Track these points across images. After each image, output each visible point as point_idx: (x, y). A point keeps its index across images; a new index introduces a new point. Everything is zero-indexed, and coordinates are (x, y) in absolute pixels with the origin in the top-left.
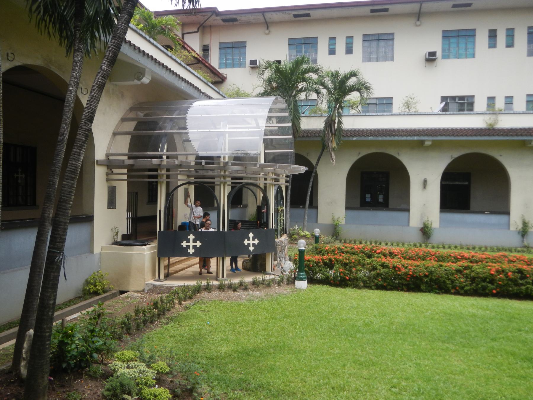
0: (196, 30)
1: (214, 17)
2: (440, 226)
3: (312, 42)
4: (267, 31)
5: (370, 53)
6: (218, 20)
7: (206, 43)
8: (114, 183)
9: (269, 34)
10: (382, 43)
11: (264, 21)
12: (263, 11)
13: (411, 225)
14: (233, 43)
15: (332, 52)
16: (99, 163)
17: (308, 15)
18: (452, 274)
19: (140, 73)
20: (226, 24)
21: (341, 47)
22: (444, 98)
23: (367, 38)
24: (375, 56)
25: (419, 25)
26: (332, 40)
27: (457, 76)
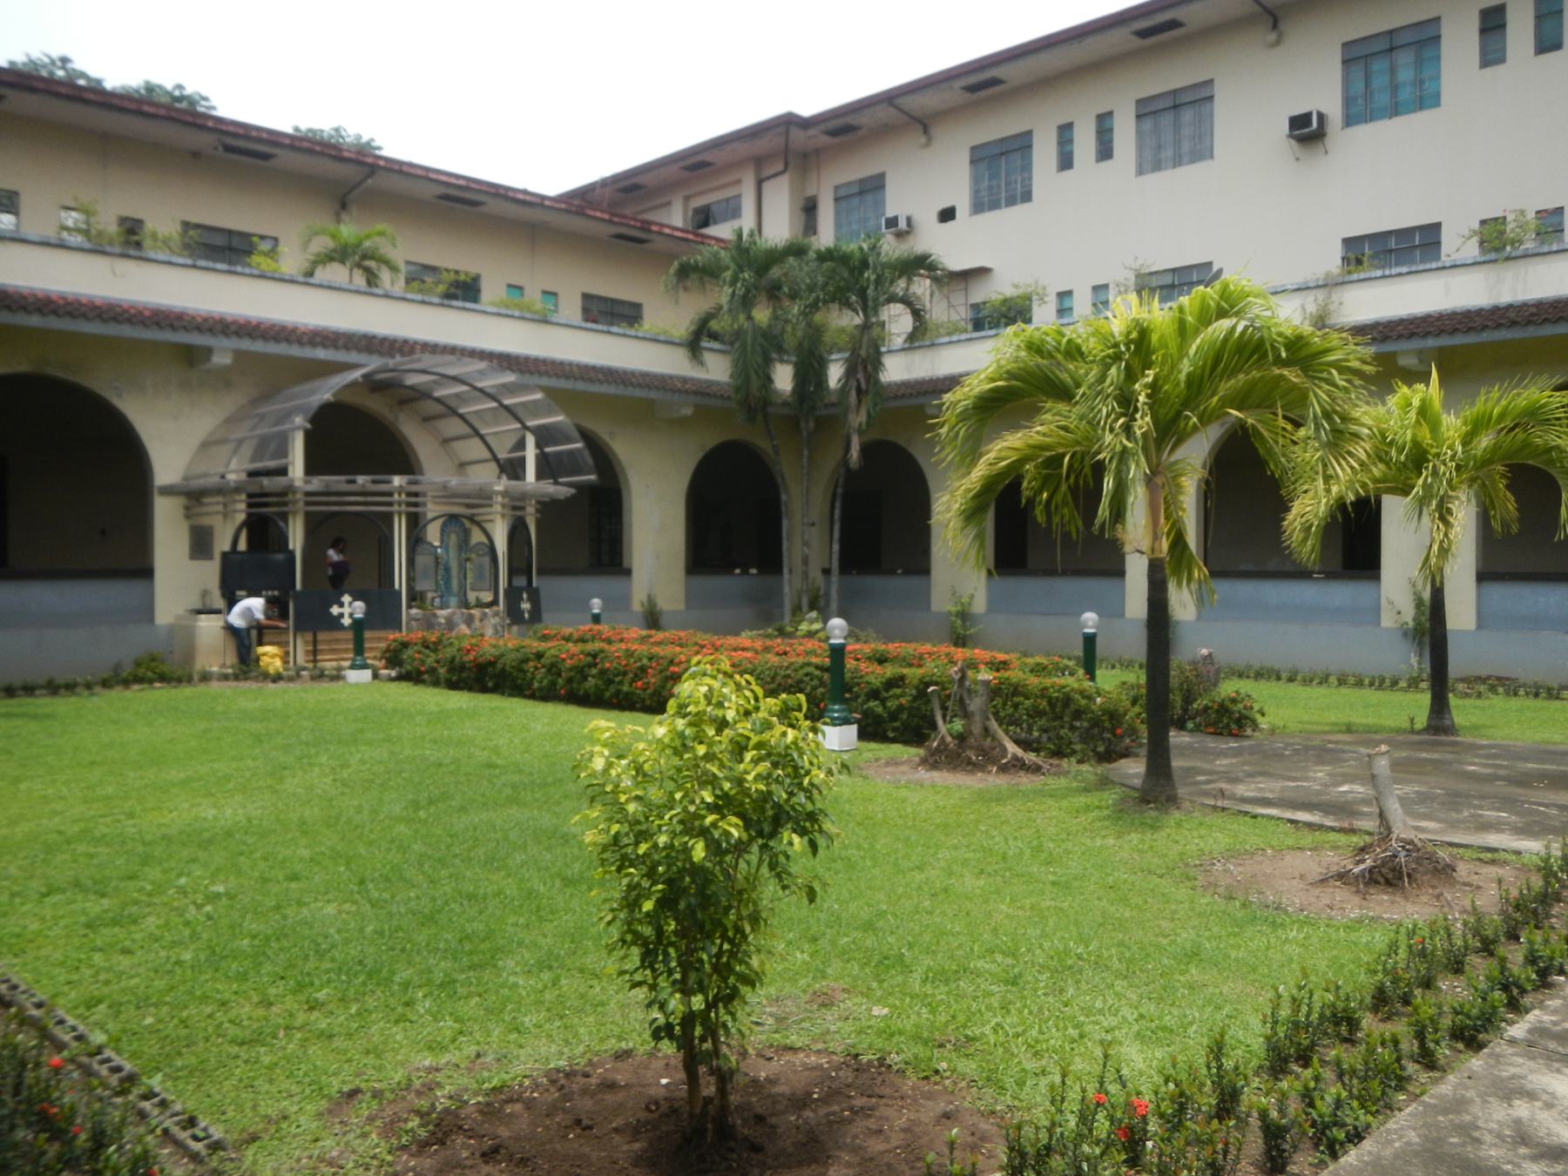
0: (781, 167)
1: (797, 136)
2: (1199, 618)
3: (1021, 145)
4: (923, 140)
5: (1159, 147)
6: (819, 138)
7: (810, 192)
8: (206, 521)
9: (928, 144)
10: (1187, 115)
11: (906, 118)
12: (889, 98)
13: (1128, 614)
14: (861, 181)
15: (1066, 162)
16: (168, 491)
17: (995, 82)
18: (526, 661)
19: (209, 351)
20: (837, 140)
21: (1085, 143)
22: (1349, 243)
23: (1147, 110)
24: (1168, 153)
25: (1278, 43)
26: (1065, 131)
27: (1392, 171)
